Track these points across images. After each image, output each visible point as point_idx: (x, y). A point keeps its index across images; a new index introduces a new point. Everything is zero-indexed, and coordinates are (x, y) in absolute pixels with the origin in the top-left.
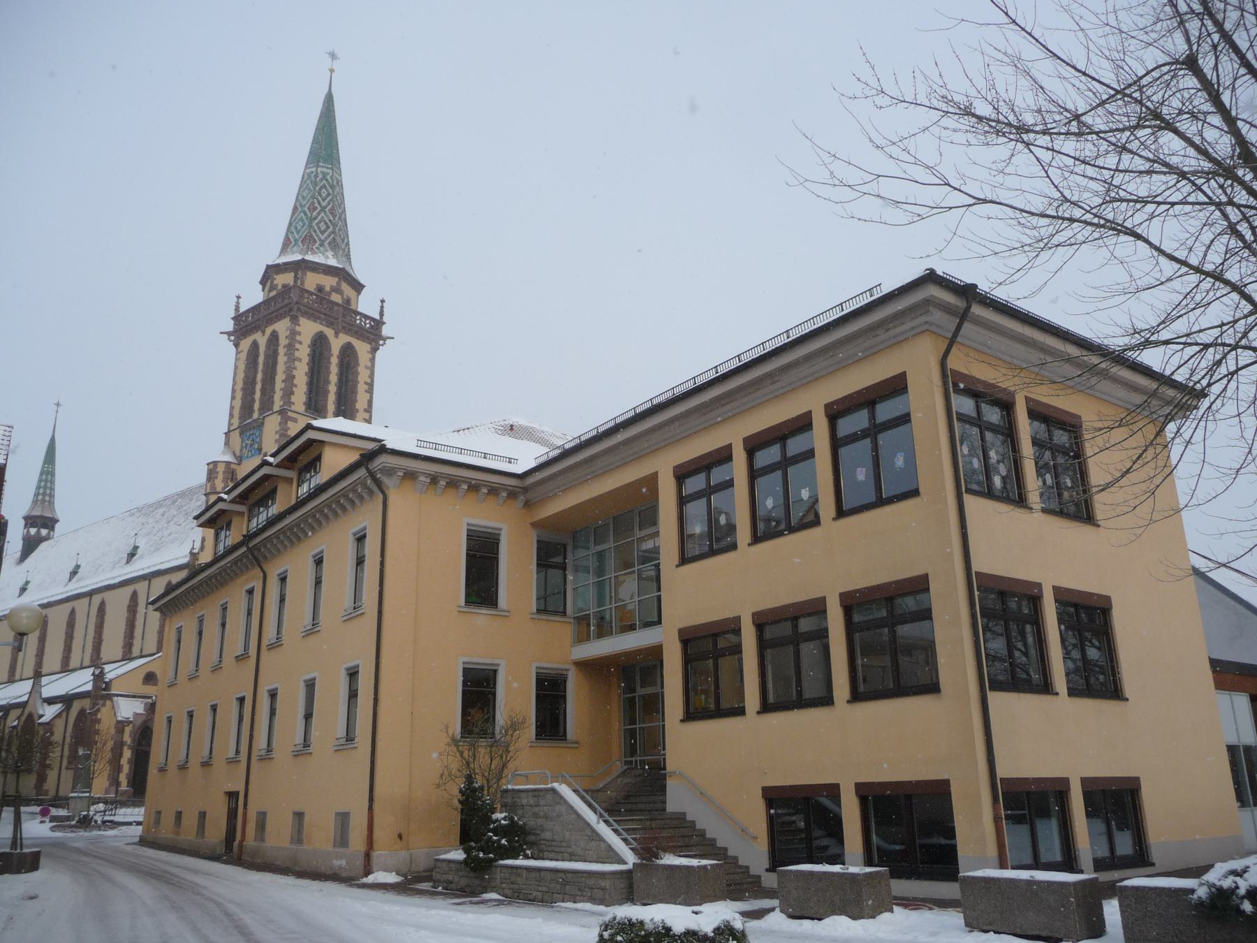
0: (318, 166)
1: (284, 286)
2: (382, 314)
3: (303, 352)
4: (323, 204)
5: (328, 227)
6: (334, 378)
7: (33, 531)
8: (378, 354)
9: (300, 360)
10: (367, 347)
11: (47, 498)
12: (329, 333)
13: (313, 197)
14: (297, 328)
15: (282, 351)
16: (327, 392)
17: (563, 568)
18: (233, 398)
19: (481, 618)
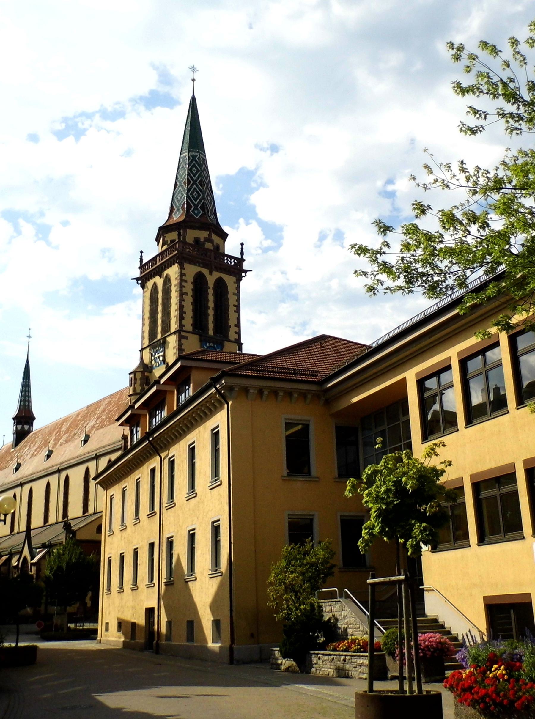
1: (172, 241)
2: (242, 253)
3: (189, 288)
6: (211, 304)
7: (19, 427)
8: (242, 283)
9: (187, 294)
10: (234, 279)
11: (27, 403)
12: (205, 272)
13: (189, 174)
16: (207, 315)
17: (356, 444)
18: (143, 325)
19: (299, 484)
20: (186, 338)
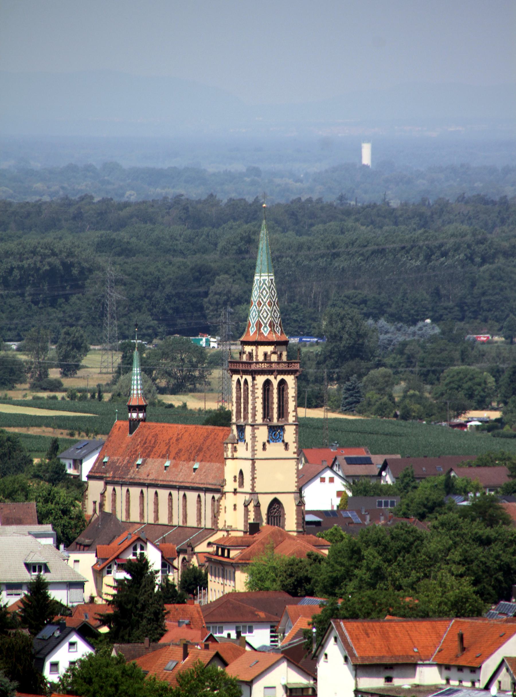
0: (261, 276)
3: (259, 393)
4: (265, 300)
5: (268, 314)
6: (275, 400)
13: (260, 297)
14: (255, 382)
15: (250, 393)
16: (272, 409)
20: (258, 429)
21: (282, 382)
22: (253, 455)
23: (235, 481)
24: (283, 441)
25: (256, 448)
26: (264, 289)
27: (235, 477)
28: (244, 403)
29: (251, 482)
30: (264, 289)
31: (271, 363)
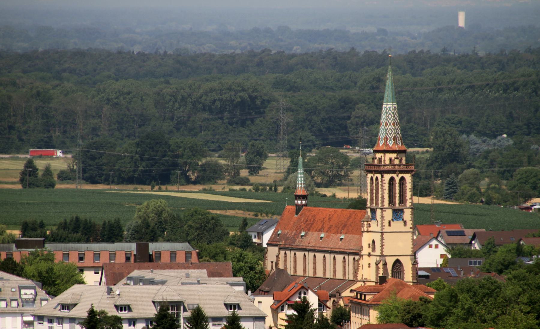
0: (387, 105)
3: (386, 186)
6: (397, 191)
14: (383, 179)
15: (380, 186)
16: (395, 197)
21: (402, 179)
22: (382, 229)
23: (369, 247)
24: (403, 220)
25: (384, 224)
26: (390, 114)
27: (369, 245)
28: (376, 193)
29: (380, 248)
30: (390, 114)
31: (395, 165)
